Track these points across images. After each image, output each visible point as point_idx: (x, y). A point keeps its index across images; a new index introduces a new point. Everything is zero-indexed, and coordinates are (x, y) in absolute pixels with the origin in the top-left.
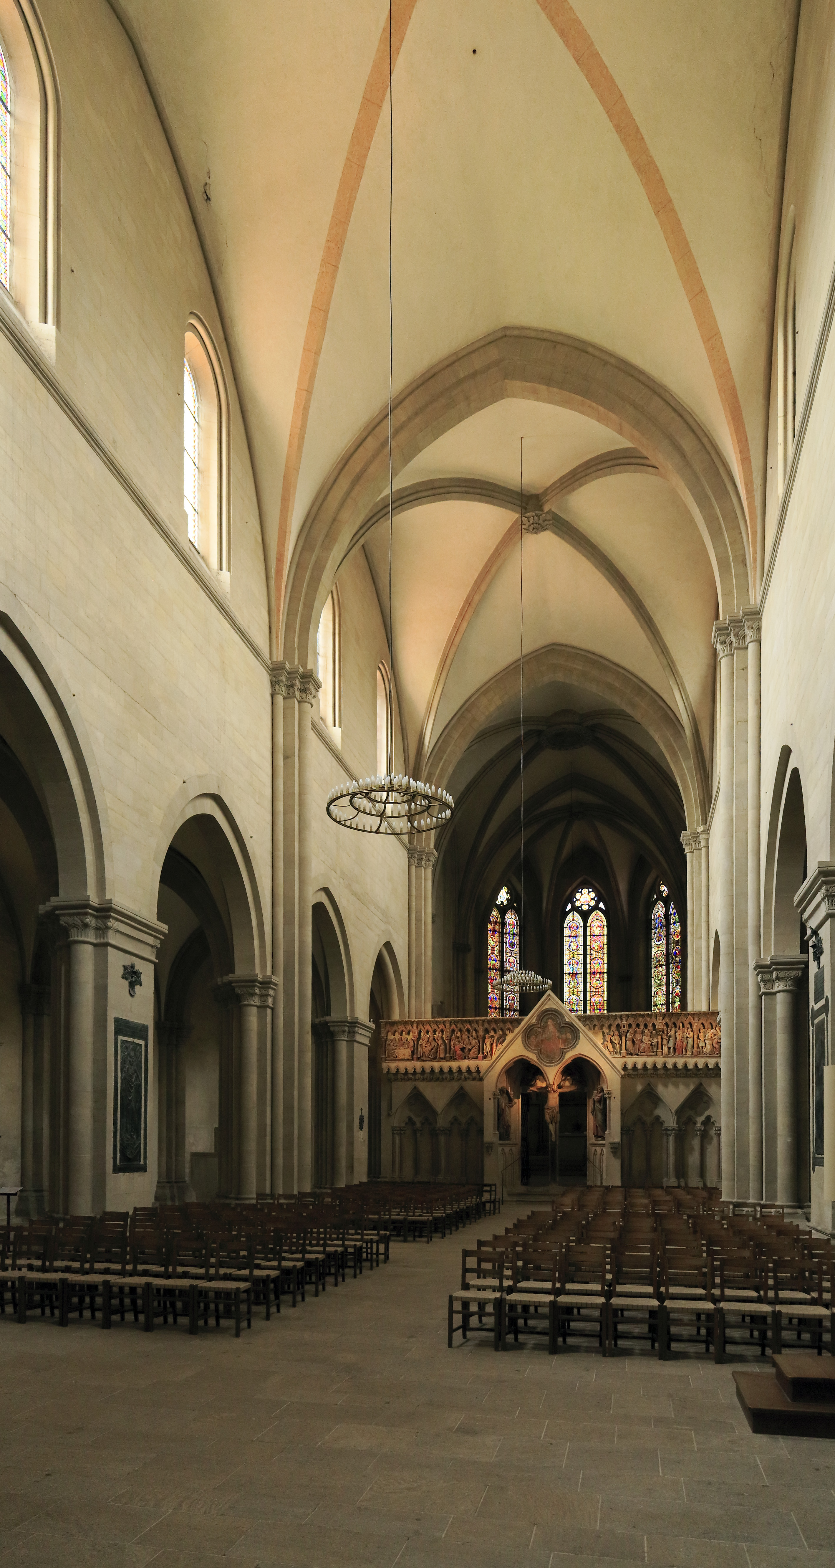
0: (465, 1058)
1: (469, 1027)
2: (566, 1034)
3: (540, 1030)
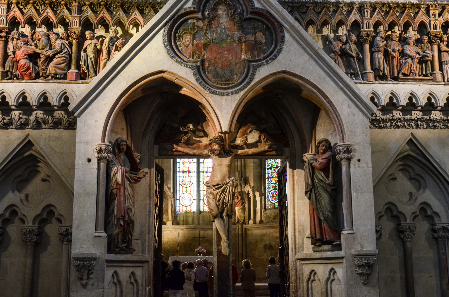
0: (37, 76)
1: (51, 14)
2: (254, 34)
3: (200, 24)
